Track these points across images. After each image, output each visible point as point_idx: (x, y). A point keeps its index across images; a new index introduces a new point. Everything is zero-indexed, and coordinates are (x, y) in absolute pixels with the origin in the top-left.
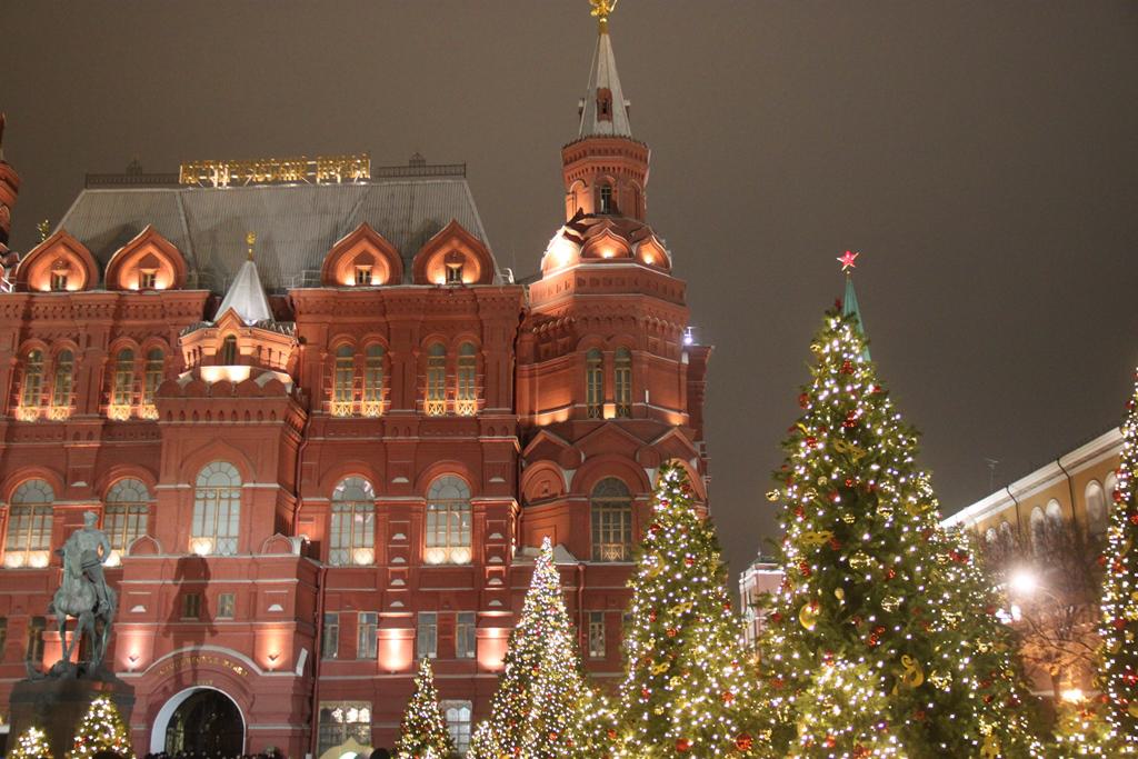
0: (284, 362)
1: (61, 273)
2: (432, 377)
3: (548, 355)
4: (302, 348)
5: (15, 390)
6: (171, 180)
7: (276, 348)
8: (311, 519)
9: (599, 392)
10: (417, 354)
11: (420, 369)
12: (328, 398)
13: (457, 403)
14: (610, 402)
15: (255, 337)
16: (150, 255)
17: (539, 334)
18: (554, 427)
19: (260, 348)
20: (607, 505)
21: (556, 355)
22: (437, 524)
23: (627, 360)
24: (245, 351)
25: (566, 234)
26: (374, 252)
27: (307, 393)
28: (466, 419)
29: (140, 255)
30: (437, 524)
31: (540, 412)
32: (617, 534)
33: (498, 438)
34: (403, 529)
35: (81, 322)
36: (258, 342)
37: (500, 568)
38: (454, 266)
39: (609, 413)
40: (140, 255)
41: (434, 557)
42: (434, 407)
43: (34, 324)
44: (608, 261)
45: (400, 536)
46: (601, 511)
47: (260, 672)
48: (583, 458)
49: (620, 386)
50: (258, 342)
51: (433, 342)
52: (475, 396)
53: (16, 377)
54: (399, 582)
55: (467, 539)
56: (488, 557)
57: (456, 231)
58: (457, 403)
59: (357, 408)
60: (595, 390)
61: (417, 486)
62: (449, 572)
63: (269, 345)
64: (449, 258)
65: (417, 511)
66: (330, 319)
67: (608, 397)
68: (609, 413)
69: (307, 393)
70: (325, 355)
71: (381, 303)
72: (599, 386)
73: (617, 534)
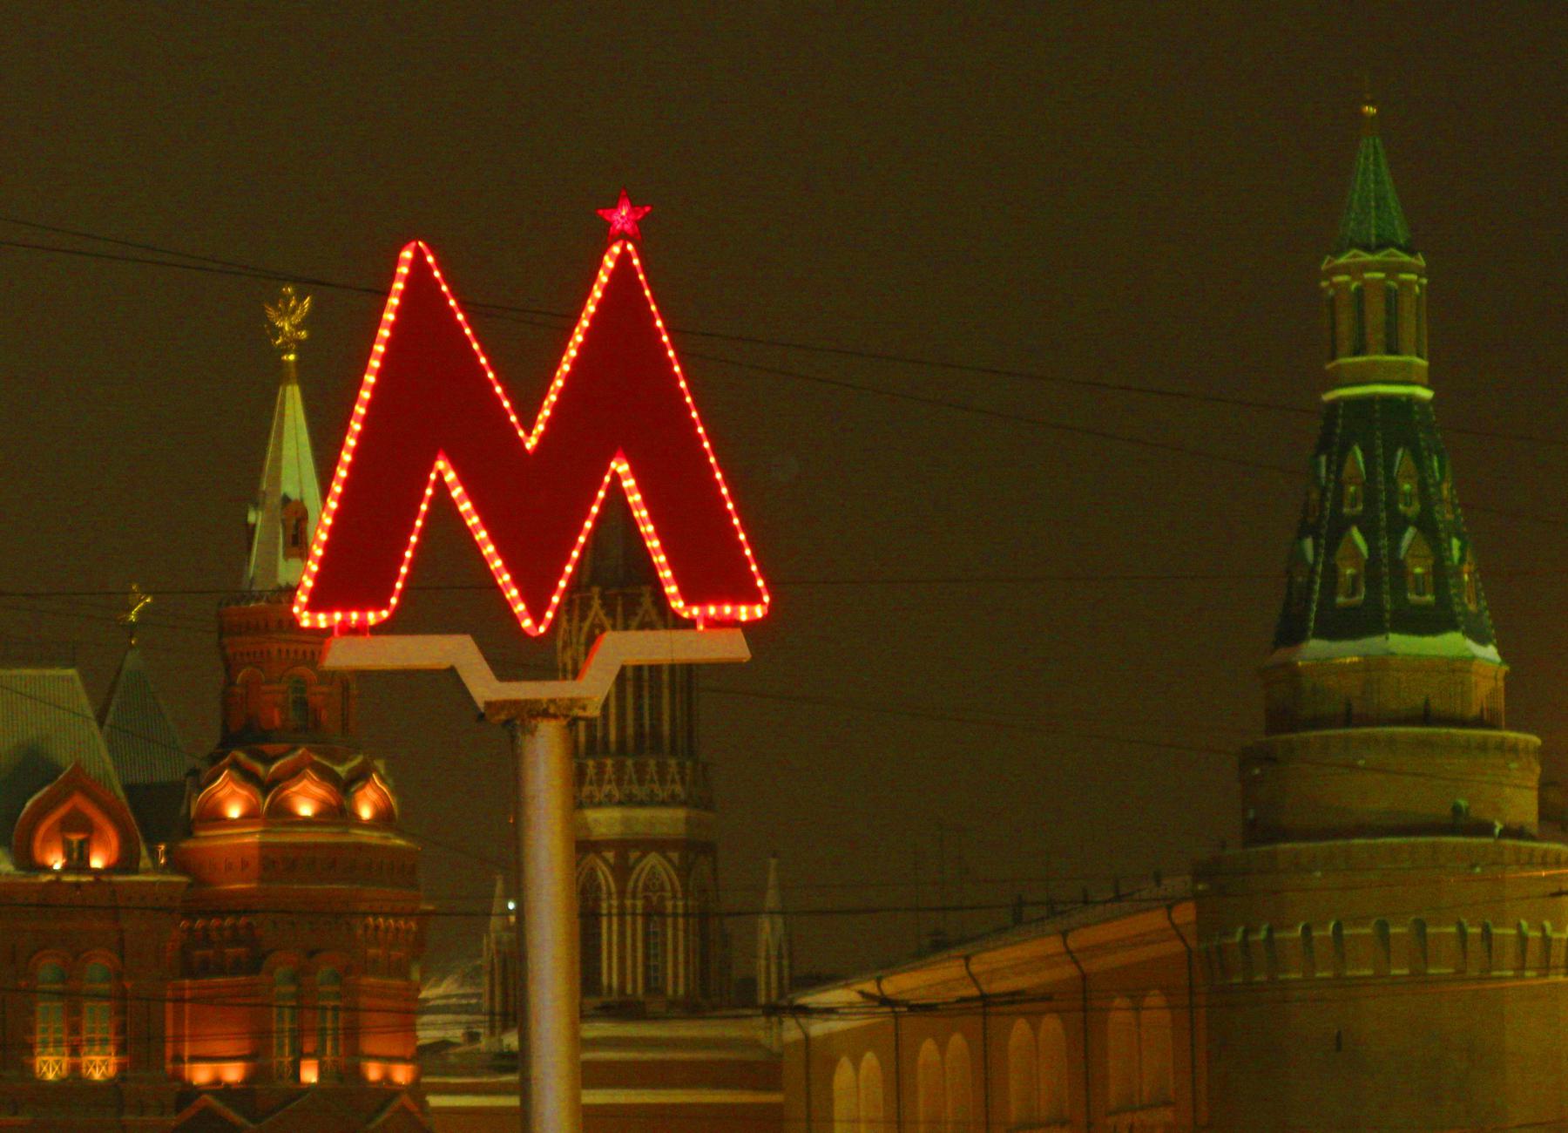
2: (49, 1019)
3: (206, 969)
13: (84, 1060)
14: (310, 1056)
17: (190, 930)
18: (219, 1089)
21: (221, 972)
23: (336, 988)
25: (236, 765)
31: (196, 1059)
38: (75, 838)
39: (310, 1075)
42: (50, 1067)
44: (306, 822)
51: (47, 970)
52: (112, 1049)
57: (79, 782)
58: (84, 1060)
64: (67, 825)
67: (308, 1048)
68: (310, 1075)
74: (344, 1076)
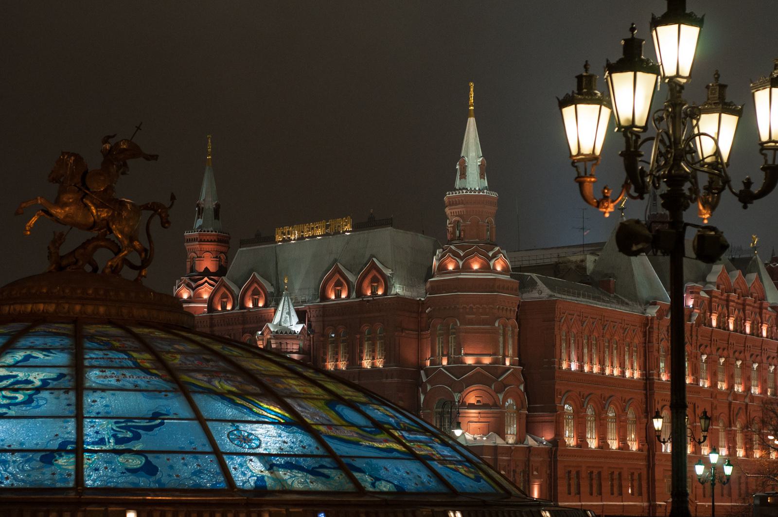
0: (295, 347)
1: (225, 300)
6: (272, 240)
10: (358, 336)
11: (361, 345)
12: (325, 361)
16: (256, 288)
19: (281, 343)
29: (252, 288)
35: (230, 327)
36: (278, 341)
59: (336, 366)
63: (288, 341)
67: (445, 353)
70: (322, 339)
71: (342, 309)
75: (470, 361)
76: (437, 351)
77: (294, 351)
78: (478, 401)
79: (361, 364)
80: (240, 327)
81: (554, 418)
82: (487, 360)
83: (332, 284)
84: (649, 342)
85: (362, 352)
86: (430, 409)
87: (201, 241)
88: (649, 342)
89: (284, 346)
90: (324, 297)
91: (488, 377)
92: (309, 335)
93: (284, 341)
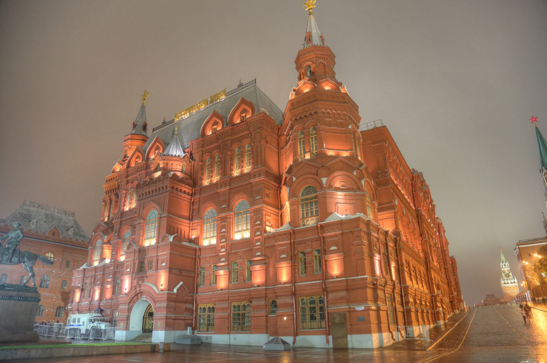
0: (179, 168)
4: (193, 162)
5: (125, 201)
7: (176, 163)
8: (196, 229)
9: (304, 150)
10: (229, 153)
11: (232, 159)
12: (203, 179)
15: (164, 160)
19: (167, 164)
20: (307, 199)
22: (238, 222)
24: (161, 166)
26: (218, 120)
27: (192, 179)
28: (248, 174)
29: (155, 146)
30: (238, 222)
32: (312, 212)
33: (257, 179)
34: (223, 227)
36: (166, 162)
37: (260, 237)
40: (155, 146)
41: (237, 237)
42: (236, 173)
43: (129, 178)
45: (224, 230)
46: (304, 202)
47: (157, 292)
48: (294, 179)
49: (313, 144)
50: (166, 162)
53: (126, 197)
54: (223, 250)
55: (249, 227)
56: (255, 233)
60: (302, 149)
61: (229, 208)
62: (244, 242)
65: (230, 218)
66: (201, 149)
67: (307, 150)
69: (192, 179)
70: (200, 163)
72: (303, 147)
73: (312, 212)
74: (320, 156)
75: (331, 153)
76: (299, 152)
77: (178, 170)
78: (343, 186)
79: (231, 174)
80: (144, 172)
81: (393, 214)
82: (345, 154)
83: (210, 125)
84: (415, 191)
85: (232, 165)
86: (296, 197)
87: (132, 139)
88: (415, 191)
89: (169, 166)
90: (203, 134)
91: (348, 165)
92: (190, 162)
93: (170, 163)
